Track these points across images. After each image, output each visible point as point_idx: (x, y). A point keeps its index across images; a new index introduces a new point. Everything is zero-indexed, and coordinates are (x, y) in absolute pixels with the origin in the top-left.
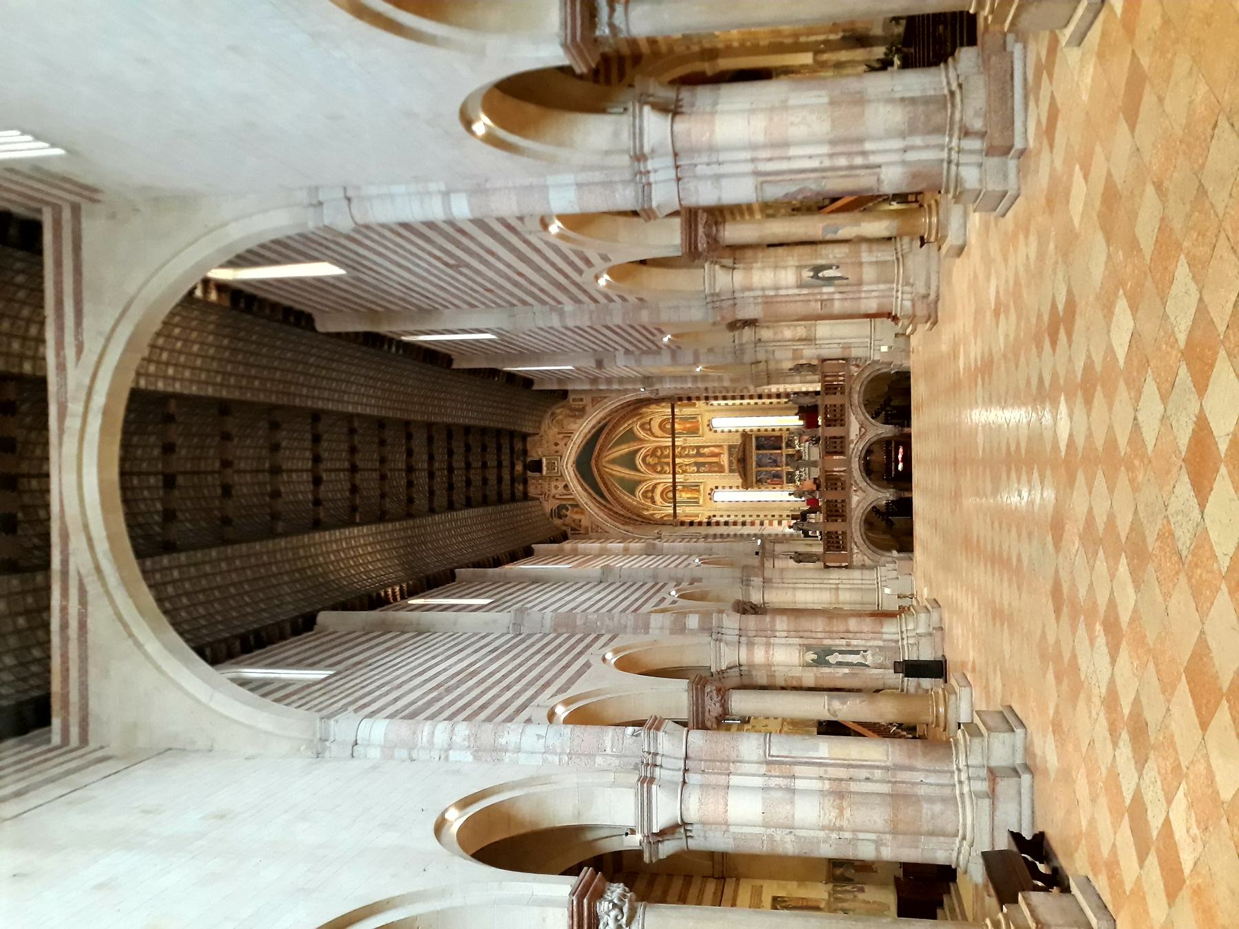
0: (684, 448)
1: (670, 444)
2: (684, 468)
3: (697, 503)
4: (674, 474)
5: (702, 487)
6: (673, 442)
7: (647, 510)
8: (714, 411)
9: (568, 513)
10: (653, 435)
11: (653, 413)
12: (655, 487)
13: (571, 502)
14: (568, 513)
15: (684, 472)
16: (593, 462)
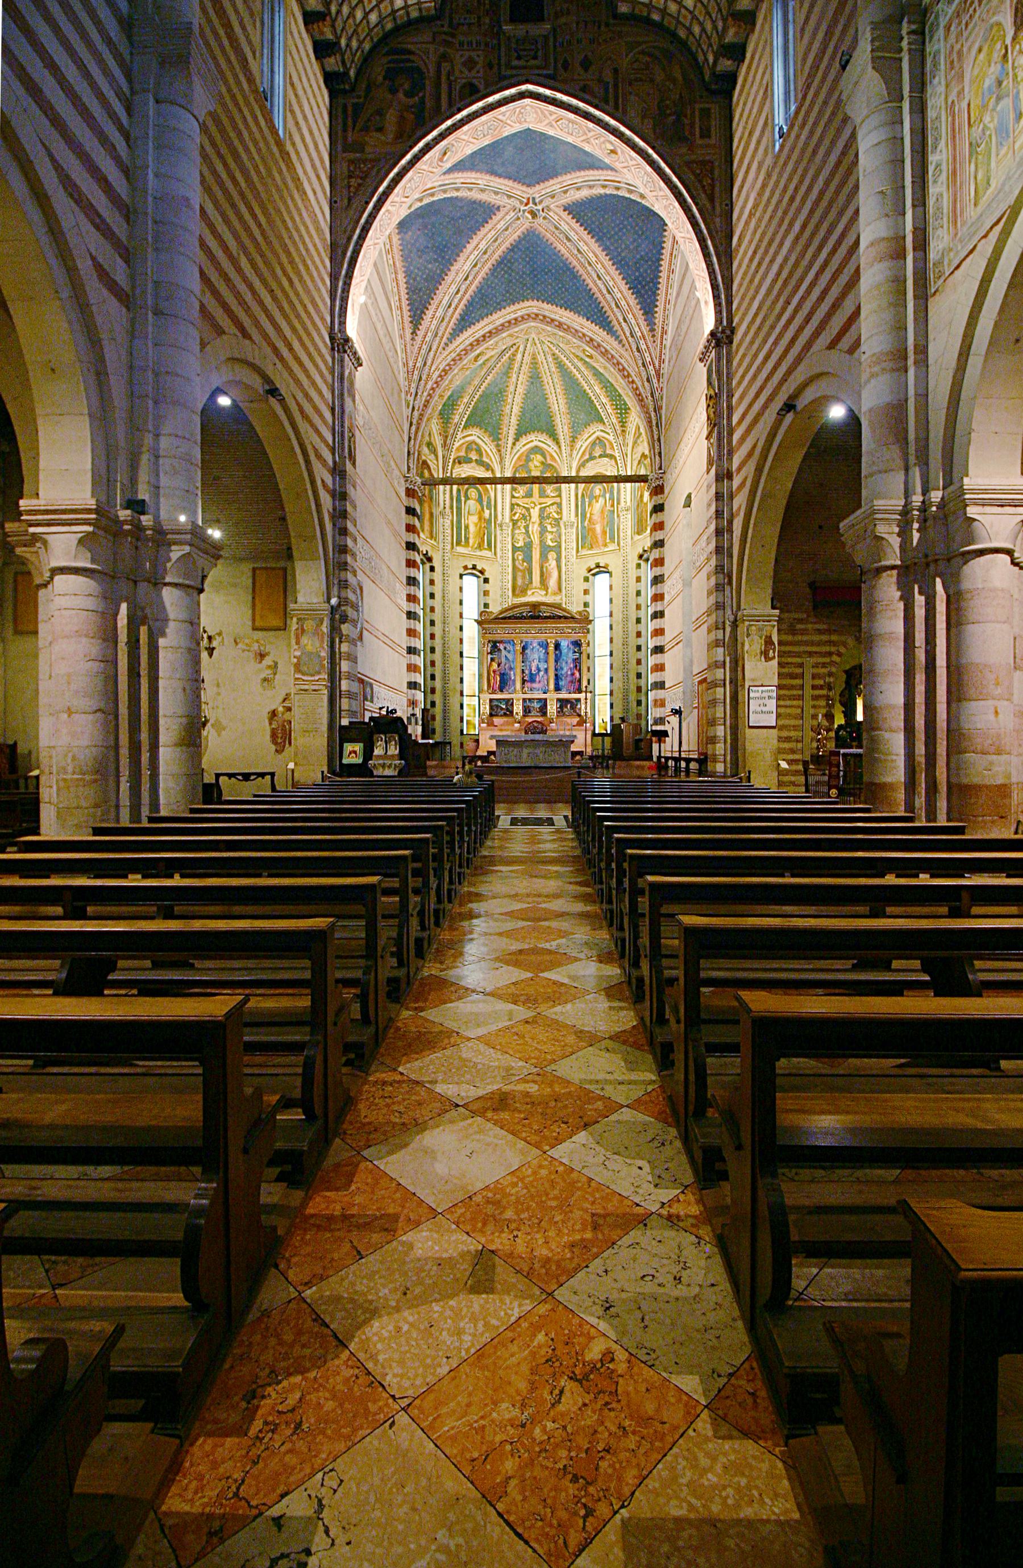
0: (557, 522)
1: (565, 473)
2: (522, 524)
3: (459, 543)
4: (513, 481)
5: (486, 553)
6: (567, 480)
7: (444, 445)
8: (625, 571)
9: (401, 95)
10: (583, 465)
11: (624, 455)
12: (488, 467)
13: (429, 104)
14: (401, 95)
15: (515, 523)
16: (532, 306)
